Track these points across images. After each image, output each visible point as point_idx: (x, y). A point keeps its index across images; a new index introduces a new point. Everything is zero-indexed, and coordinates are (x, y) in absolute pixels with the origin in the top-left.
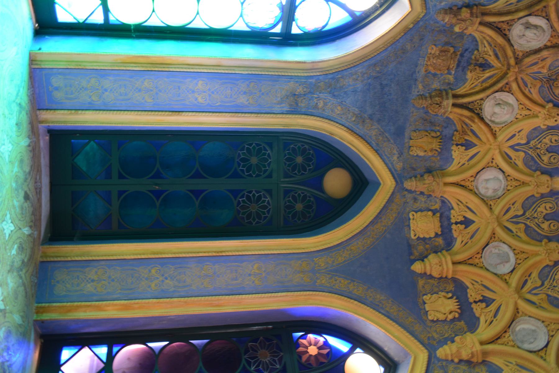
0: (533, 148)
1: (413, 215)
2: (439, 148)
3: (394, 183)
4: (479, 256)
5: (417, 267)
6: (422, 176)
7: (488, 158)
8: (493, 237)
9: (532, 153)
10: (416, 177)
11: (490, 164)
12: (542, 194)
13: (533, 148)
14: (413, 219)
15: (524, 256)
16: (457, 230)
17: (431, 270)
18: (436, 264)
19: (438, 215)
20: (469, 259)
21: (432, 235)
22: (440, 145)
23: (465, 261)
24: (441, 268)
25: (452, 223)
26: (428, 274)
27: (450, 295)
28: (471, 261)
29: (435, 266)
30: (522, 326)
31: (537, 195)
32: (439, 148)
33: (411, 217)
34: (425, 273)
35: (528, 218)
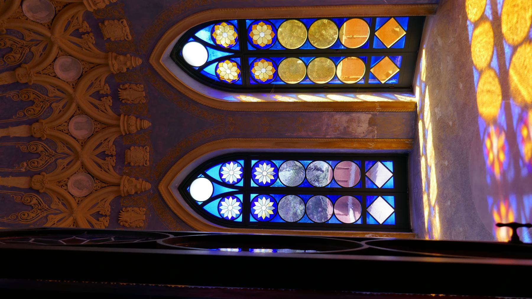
0: (44, 210)
1: (146, 164)
2: (121, 213)
3: (159, 188)
4: (96, 130)
5: (146, 124)
6: (136, 193)
8: (83, 143)
9: (45, 206)
10: (142, 192)
11: (80, 200)
12: (39, 174)
13: (44, 210)
14: (146, 161)
15: (61, 128)
16: (112, 150)
17: (136, 121)
19: (126, 163)
20: (105, 128)
21: (132, 148)
22: (121, 215)
23: (108, 127)
24: (129, 122)
25: (115, 156)
28: (104, 126)
30: (71, 75)
31: (44, 173)
32: (121, 213)
33: (148, 162)
34: (141, 120)
35: (53, 156)
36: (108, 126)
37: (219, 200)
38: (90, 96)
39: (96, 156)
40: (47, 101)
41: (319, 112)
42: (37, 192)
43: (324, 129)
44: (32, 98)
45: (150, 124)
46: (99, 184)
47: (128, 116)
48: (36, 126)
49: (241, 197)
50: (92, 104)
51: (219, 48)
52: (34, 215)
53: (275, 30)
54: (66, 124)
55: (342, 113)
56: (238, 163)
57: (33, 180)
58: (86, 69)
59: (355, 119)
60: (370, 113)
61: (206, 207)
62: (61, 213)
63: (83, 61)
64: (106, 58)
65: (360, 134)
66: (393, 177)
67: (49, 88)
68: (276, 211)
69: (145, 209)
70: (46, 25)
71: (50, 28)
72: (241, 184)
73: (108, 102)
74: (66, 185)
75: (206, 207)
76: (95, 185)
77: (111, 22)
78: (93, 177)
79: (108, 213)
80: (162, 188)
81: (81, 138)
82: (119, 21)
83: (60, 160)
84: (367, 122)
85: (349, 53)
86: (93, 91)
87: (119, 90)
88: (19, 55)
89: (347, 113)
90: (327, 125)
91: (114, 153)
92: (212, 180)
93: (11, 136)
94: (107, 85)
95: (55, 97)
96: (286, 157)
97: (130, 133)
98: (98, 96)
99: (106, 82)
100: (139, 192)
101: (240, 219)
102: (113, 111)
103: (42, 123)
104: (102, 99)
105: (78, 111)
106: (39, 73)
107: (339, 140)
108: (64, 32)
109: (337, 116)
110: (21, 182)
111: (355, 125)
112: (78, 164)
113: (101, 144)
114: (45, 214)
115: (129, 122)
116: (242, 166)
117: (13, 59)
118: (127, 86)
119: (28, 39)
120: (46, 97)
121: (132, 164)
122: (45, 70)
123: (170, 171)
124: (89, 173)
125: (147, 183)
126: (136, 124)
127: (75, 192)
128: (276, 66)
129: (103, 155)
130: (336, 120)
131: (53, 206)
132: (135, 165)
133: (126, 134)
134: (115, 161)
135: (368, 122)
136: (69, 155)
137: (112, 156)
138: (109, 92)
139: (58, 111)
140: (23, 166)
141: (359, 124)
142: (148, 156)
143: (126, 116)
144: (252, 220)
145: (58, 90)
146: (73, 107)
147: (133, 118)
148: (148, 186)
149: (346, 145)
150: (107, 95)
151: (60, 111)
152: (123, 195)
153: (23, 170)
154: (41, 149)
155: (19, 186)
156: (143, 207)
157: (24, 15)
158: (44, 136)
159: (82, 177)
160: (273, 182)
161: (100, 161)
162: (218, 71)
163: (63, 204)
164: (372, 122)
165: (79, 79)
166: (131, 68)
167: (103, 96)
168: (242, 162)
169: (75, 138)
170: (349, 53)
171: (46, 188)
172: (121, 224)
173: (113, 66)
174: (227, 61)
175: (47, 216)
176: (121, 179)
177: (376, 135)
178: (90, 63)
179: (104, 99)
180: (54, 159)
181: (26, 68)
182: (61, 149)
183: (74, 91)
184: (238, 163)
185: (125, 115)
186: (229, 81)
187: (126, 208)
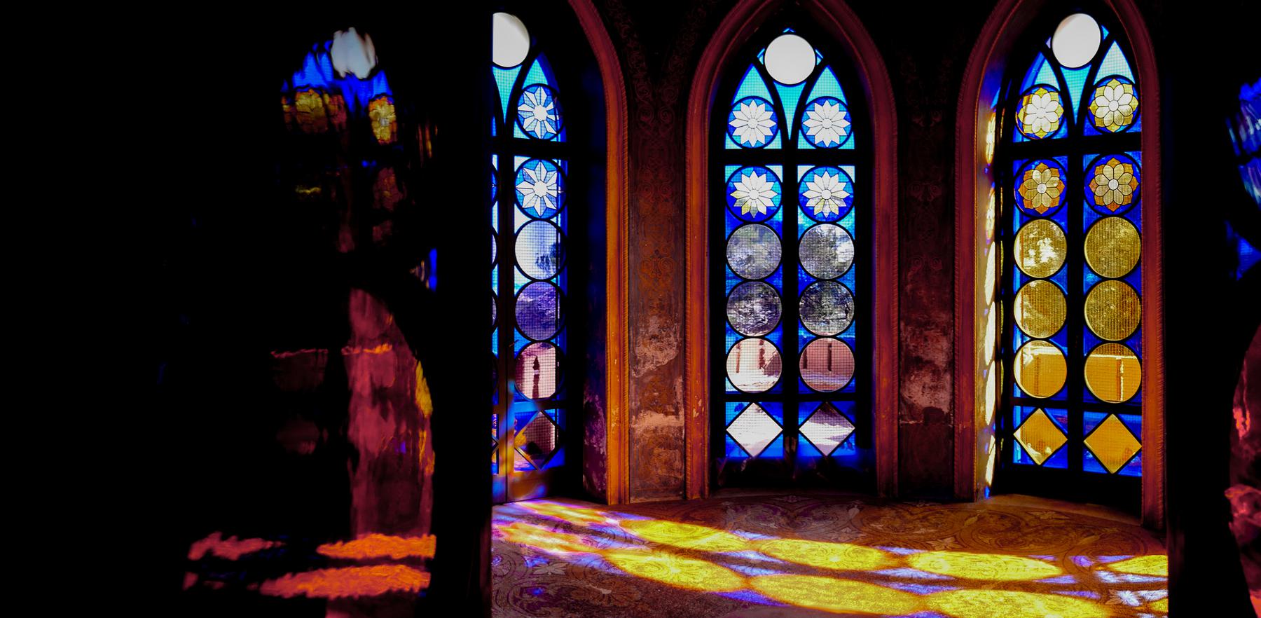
37: (768, 97)
49: (777, 144)
51: (1089, 90)
55: (952, 353)
56: (849, 136)
59: (938, 380)
60: (950, 410)
61: (753, 73)
65: (909, 390)
66: (820, 455)
68: (748, 220)
72: (802, 144)
75: (753, 73)
84: (933, 405)
85: (1075, 364)
89: (952, 365)
92: (811, 82)
101: (730, 145)
107: (896, 347)
109: (944, 344)
111: (927, 379)
130: (938, 341)
135: (934, 406)
141: (930, 388)
144: (729, 170)
149: (885, 360)
160: (809, 213)
168: (850, 145)
170: (1075, 364)
177: (906, 422)
184: (849, 136)
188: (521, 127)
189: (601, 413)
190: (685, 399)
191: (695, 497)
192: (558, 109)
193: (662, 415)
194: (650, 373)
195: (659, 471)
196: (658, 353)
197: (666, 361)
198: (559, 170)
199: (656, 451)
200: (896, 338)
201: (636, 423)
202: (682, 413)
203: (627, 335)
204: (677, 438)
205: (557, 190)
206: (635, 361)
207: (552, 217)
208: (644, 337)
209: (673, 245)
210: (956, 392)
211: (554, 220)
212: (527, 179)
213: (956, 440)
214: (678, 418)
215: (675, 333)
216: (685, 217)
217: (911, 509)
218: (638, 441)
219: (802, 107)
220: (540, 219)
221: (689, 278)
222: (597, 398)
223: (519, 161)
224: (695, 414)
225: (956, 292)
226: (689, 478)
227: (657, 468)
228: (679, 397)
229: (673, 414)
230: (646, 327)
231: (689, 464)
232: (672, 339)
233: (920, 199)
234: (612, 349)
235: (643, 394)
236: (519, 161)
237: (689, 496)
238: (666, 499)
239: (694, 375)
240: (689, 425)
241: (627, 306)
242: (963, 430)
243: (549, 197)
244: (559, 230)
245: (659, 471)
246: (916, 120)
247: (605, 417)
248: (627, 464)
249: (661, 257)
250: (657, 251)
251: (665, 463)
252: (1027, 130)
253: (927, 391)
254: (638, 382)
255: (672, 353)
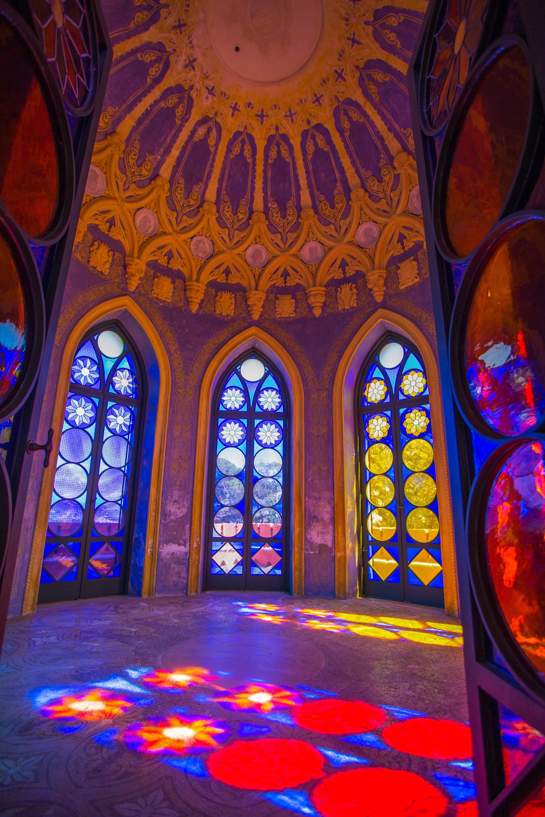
1: (278, 314)
3: (254, 327)
5: (317, 312)
6: (249, 306)
7: (238, 259)
11: (242, 256)
12: (266, 219)
18: (315, 298)
19: (278, 296)
21: (293, 301)
24: (318, 295)
26: (322, 305)
27: (339, 289)
28: (314, 273)
29: (317, 299)
30: (361, 239)
33: (279, 316)
34: (322, 307)
35: (284, 230)
36: (314, 278)
38: (343, 259)
39: (285, 269)
40: (336, 220)
41: (334, 488)
42: (250, 218)
43: (315, 495)
44: (337, 205)
45: (317, 316)
46: (257, 273)
47: (325, 295)
48: (312, 212)
50: (336, 260)
52: (228, 216)
53: (422, 436)
54: (315, 239)
56: (280, 407)
57: (260, 214)
58: (368, 251)
59: (326, 528)
62: (230, 240)
63: (376, 247)
64: (380, 268)
67: (348, 220)
69: (232, 314)
70: (407, 209)
71: (404, 212)
72: (258, 409)
73: (338, 275)
74: (257, 243)
76: (257, 269)
77: (416, 267)
78: (264, 267)
79: (229, 282)
80: (253, 330)
81: (302, 253)
82: (418, 274)
83: (280, 237)
84: (323, 542)
86: (348, 260)
87: (350, 284)
88: (376, 189)
90: (320, 498)
91: (288, 285)
93: (300, 192)
94: (355, 272)
95: (340, 227)
96: (287, 456)
97: (307, 297)
98: (344, 265)
99: (357, 271)
100: (249, 309)
101: (222, 408)
102: (329, 281)
103: (314, 217)
104: (341, 269)
105: (327, 248)
106: (361, 209)
107: (303, 510)
108: (403, 227)
109: (329, 508)
110: (258, 204)
112: (277, 252)
113: (297, 272)
114: (229, 226)
115: (318, 295)
116: (277, 410)
117: (372, 184)
118: (355, 290)
119: (392, 195)
120: (339, 219)
121: (277, 302)
122: (364, 214)
123: (270, 337)
124: (268, 262)
125: (258, 316)
126: (317, 302)
127: (250, 251)
128: (383, 440)
129: (285, 275)
131: (236, 232)
132: (276, 305)
133: (306, 294)
134: (280, 286)
136: (285, 244)
137: (285, 282)
138: (348, 275)
139: (327, 231)
140: (274, 204)
142: (286, 316)
143: (324, 293)
145: (347, 229)
146: (331, 243)
147: (323, 299)
148: (256, 316)
150: (344, 273)
151: (327, 233)
152: (246, 294)
153: (270, 205)
154: (290, 218)
155: (255, 202)
156: (234, 313)
157: (413, 187)
158: (301, 220)
159: (264, 256)
160: (260, 443)
161: (280, 272)
162: (375, 380)
163: (239, 241)
164: (322, 547)
165: (359, 246)
166: (372, 292)
167: (344, 270)
169: (301, 248)
171: (253, 225)
172: (219, 293)
173: (373, 274)
174: (386, 389)
175: (227, 228)
176: (262, 291)
178: (375, 254)
179: (340, 271)
180: (280, 231)
181: (365, 196)
182: (291, 237)
183: (346, 243)
184: (280, 407)
185: (326, 292)
186: (366, 393)
187: (235, 297)
188: (114, 387)
189: (142, 543)
190: (190, 537)
191: (192, 594)
192: (135, 381)
193: (176, 545)
194: (172, 521)
195: (173, 578)
196: (177, 510)
197: (181, 515)
198: (132, 413)
199: (173, 566)
200: (303, 506)
201: (162, 549)
202: (188, 544)
203: (161, 500)
204: (184, 559)
205: (130, 422)
206: (165, 515)
207: (126, 435)
208: (170, 501)
209: (189, 454)
210: (336, 535)
211: (126, 437)
212: (113, 413)
213: (336, 562)
214: (185, 547)
215: (187, 500)
216: (196, 440)
217: (311, 601)
218: (163, 560)
219: (258, 392)
220: (118, 435)
221: (196, 471)
222: (141, 534)
223: (110, 404)
224: (195, 545)
225: (335, 480)
226: (189, 582)
227: (172, 576)
228: (187, 536)
229: (183, 545)
230: (172, 496)
231: (190, 574)
232: (185, 503)
233: (315, 433)
234: (152, 507)
235: (167, 533)
236: (110, 404)
237: (189, 593)
238: (176, 595)
239: (195, 524)
240: (191, 551)
241: (162, 483)
242: (340, 557)
243: (125, 425)
244: (129, 443)
245: (173, 578)
246: (313, 396)
247: (145, 545)
248: (155, 573)
249: (182, 459)
250: (180, 456)
251: (177, 573)
252: (369, 400)
253: (320, 535)
254: (165, 526)
255: (185, 510)
